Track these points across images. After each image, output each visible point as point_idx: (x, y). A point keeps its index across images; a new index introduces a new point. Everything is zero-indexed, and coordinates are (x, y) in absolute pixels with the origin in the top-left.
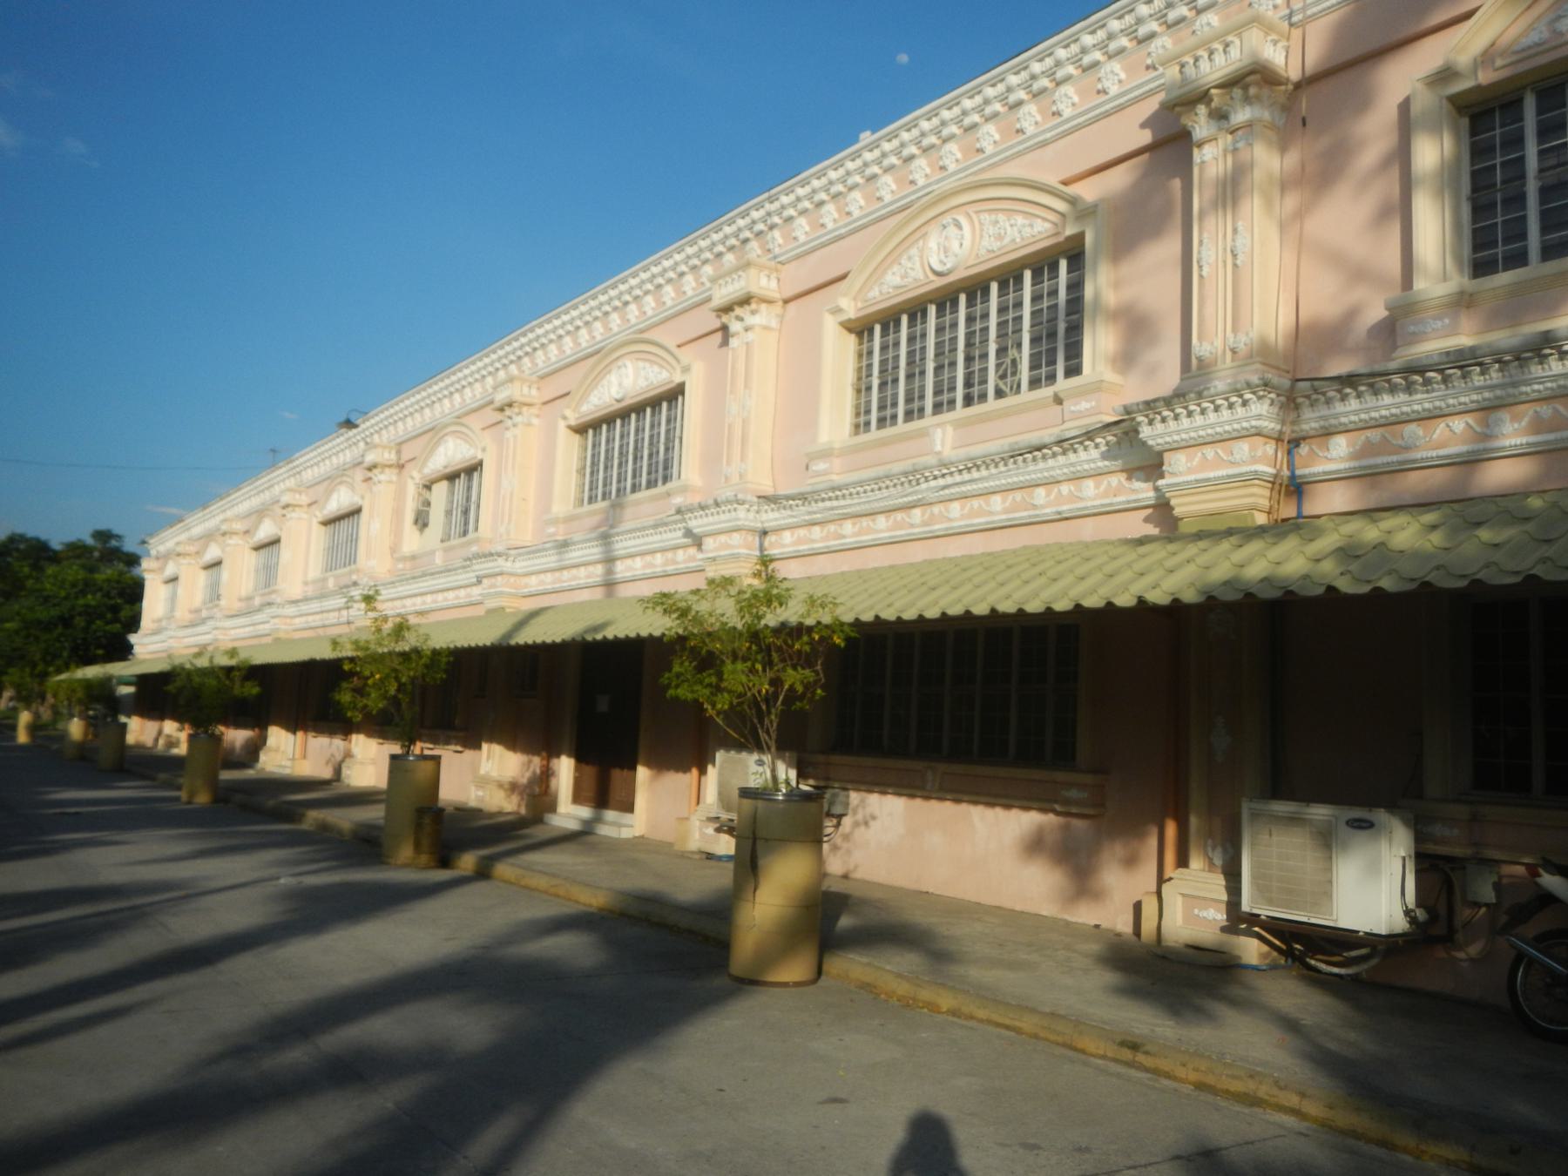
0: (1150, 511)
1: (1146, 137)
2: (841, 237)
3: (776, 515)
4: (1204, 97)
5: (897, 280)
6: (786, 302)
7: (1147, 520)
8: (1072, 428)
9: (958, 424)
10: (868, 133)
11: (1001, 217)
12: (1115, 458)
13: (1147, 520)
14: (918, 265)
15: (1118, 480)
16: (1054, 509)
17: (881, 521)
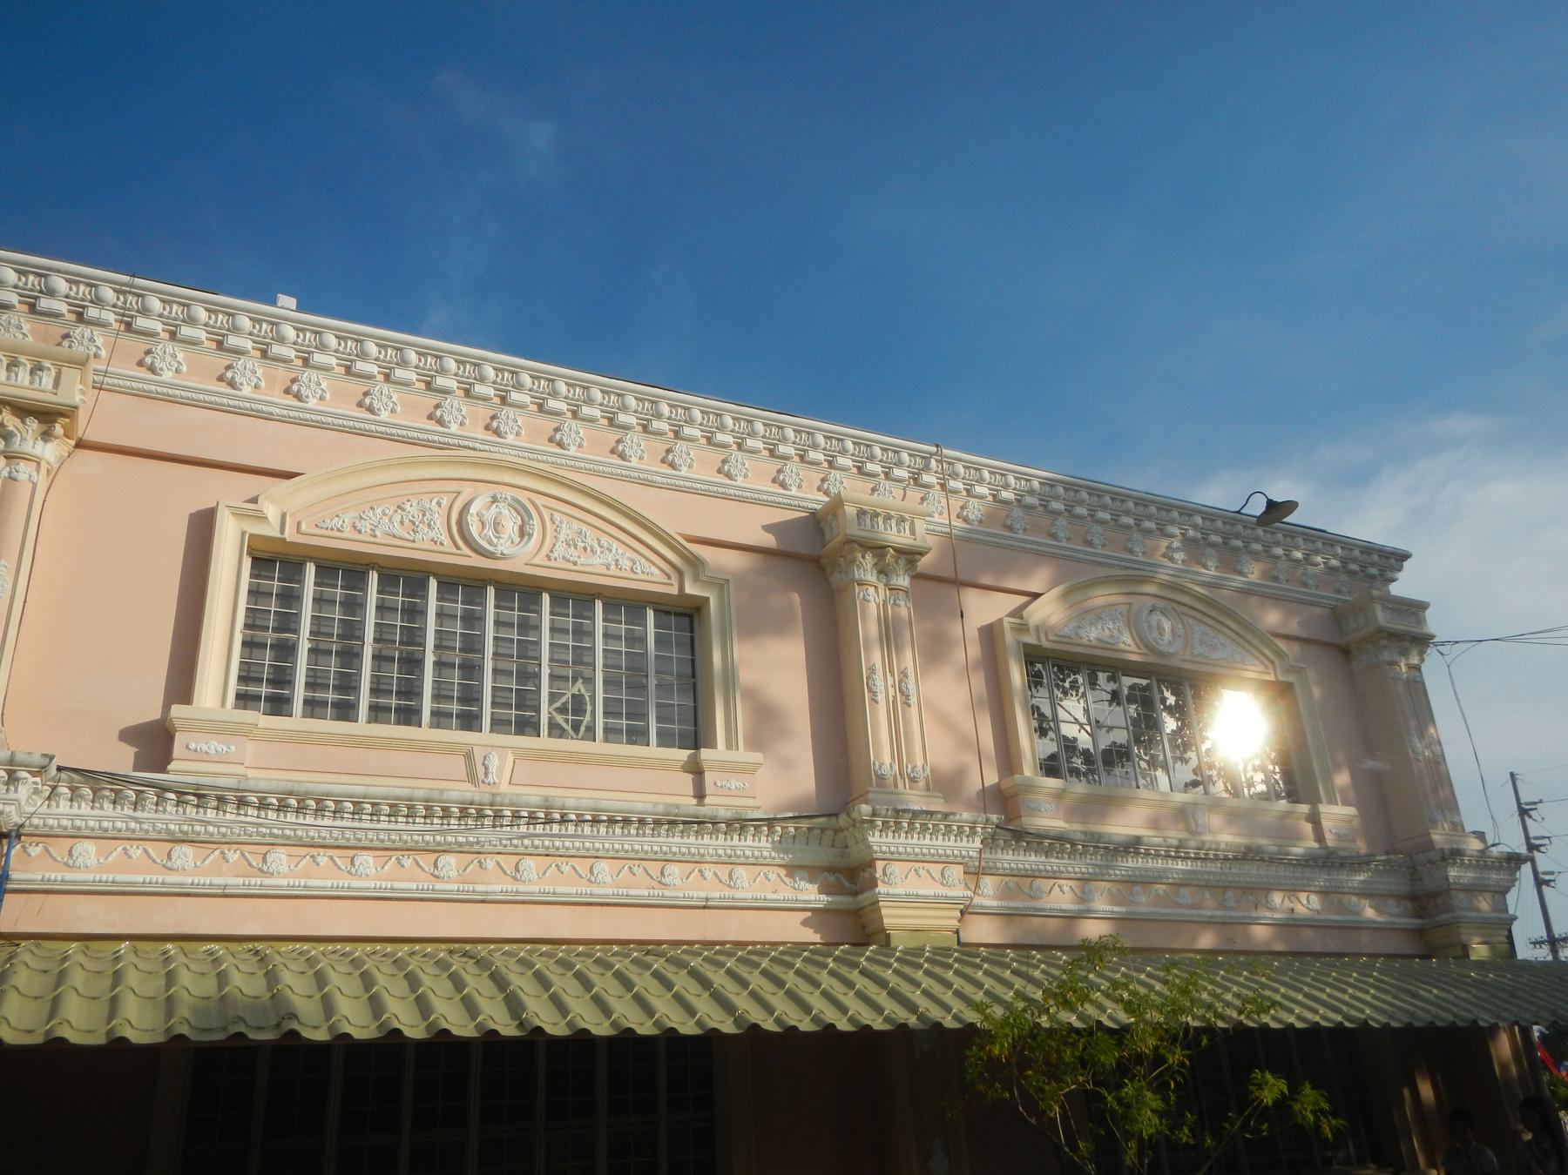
0: (809, 914)
1: (769, 540)
2: (268, 417)
3: (85, 809)
4: (879, 549)
5: (397, 529)
6: (81, 445)
7: (805, 923)
8: (718, 804)
9: (522, 755)
10: (291, 302)
11: (584, 528)
12: (786, 852)
13: (805, 923)
14: (439, 522)
15: (776, 874)
16: (703, 894)
17: (366, 860)
